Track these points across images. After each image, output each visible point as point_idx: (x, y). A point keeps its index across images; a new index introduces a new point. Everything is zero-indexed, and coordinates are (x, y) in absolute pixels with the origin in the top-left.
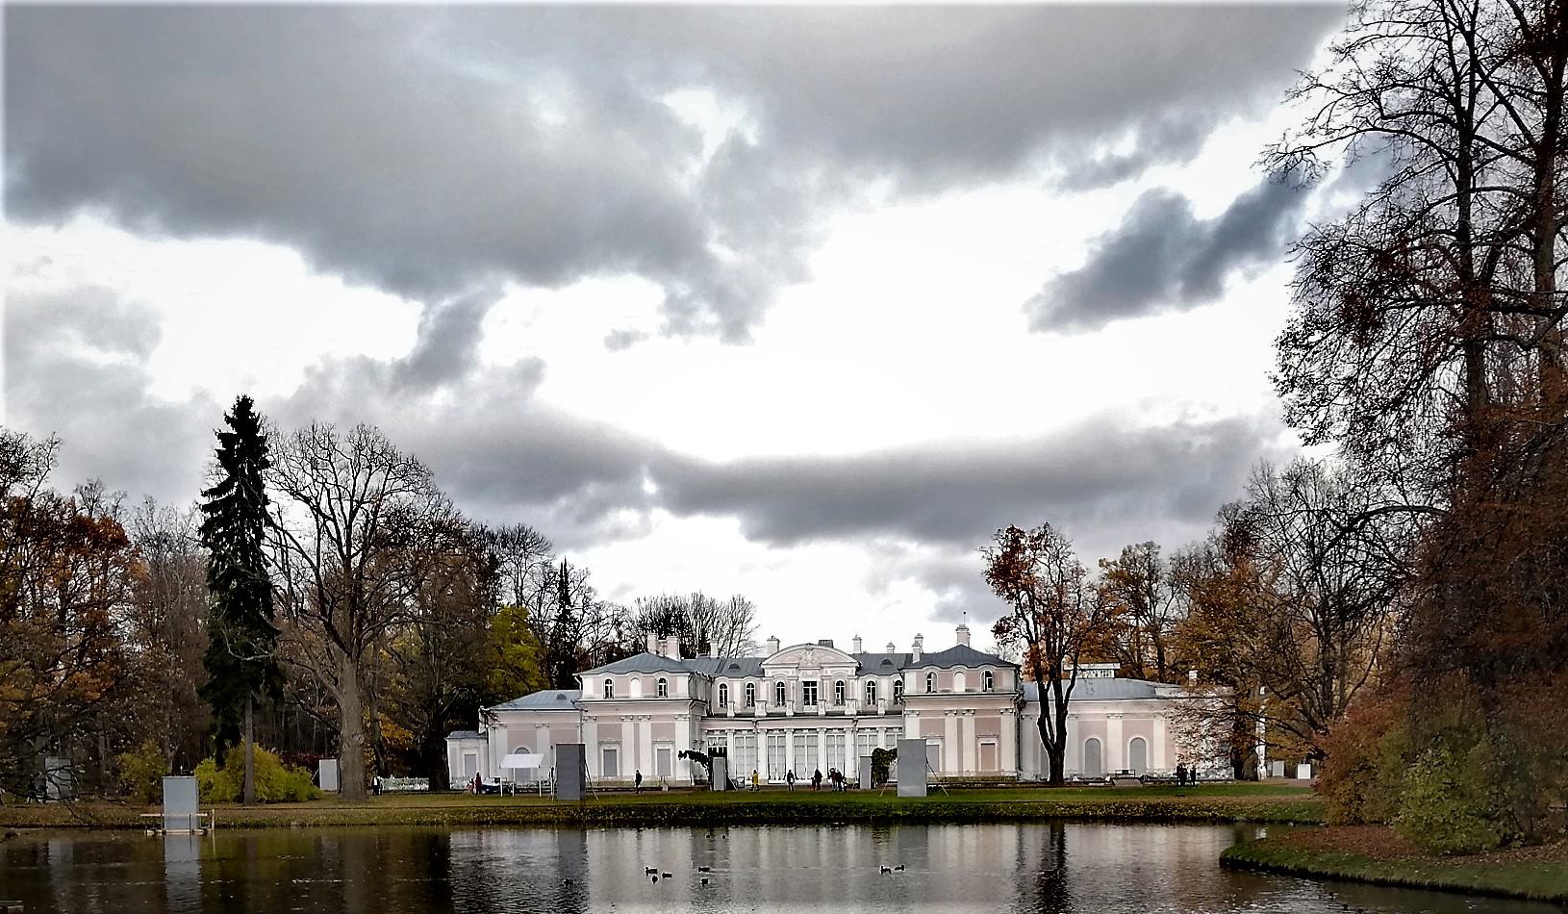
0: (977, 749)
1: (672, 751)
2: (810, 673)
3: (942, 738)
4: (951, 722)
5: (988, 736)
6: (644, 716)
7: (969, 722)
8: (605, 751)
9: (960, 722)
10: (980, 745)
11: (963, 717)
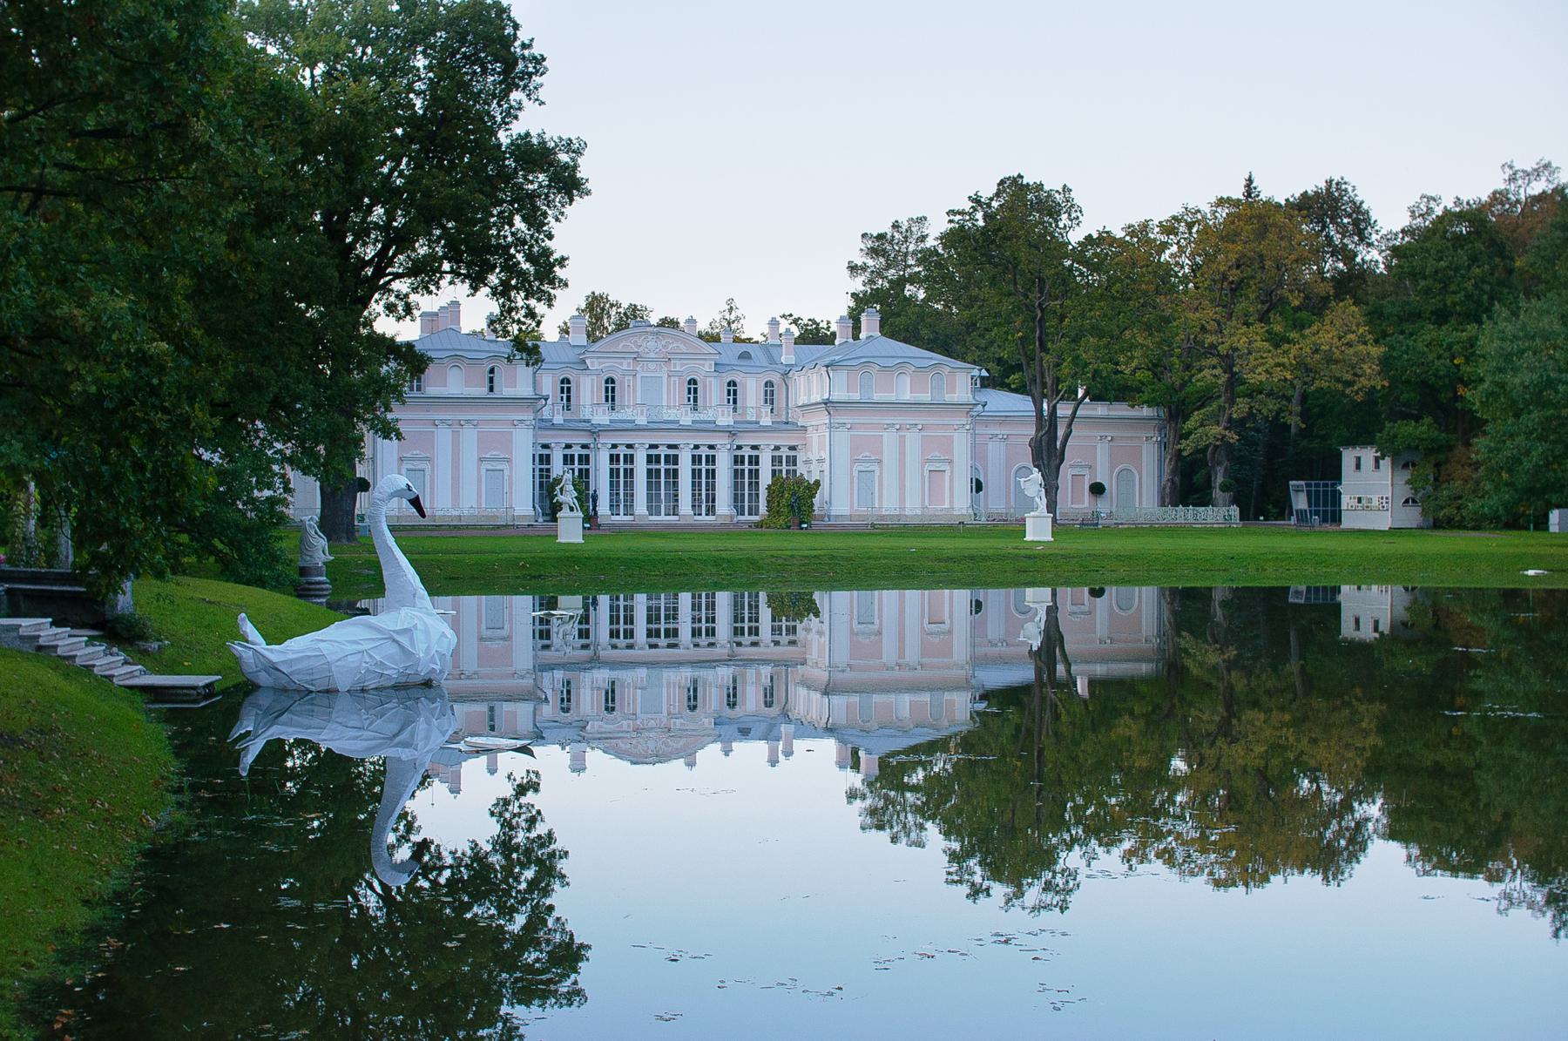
0: (923, 477)
1: (506, 473)
2: (652, 366)
3: (880, 462)
4: (889, 439)
5: (940, 461)
6: (468, 421)
7: (913, 439)
8: (487, 470)
9: (902, 440)
10: (926, 474)
11: (908, 435)
